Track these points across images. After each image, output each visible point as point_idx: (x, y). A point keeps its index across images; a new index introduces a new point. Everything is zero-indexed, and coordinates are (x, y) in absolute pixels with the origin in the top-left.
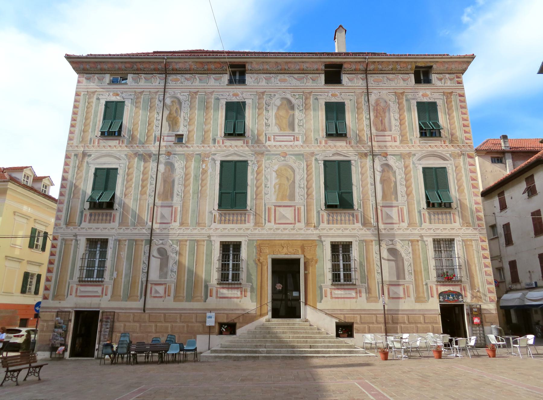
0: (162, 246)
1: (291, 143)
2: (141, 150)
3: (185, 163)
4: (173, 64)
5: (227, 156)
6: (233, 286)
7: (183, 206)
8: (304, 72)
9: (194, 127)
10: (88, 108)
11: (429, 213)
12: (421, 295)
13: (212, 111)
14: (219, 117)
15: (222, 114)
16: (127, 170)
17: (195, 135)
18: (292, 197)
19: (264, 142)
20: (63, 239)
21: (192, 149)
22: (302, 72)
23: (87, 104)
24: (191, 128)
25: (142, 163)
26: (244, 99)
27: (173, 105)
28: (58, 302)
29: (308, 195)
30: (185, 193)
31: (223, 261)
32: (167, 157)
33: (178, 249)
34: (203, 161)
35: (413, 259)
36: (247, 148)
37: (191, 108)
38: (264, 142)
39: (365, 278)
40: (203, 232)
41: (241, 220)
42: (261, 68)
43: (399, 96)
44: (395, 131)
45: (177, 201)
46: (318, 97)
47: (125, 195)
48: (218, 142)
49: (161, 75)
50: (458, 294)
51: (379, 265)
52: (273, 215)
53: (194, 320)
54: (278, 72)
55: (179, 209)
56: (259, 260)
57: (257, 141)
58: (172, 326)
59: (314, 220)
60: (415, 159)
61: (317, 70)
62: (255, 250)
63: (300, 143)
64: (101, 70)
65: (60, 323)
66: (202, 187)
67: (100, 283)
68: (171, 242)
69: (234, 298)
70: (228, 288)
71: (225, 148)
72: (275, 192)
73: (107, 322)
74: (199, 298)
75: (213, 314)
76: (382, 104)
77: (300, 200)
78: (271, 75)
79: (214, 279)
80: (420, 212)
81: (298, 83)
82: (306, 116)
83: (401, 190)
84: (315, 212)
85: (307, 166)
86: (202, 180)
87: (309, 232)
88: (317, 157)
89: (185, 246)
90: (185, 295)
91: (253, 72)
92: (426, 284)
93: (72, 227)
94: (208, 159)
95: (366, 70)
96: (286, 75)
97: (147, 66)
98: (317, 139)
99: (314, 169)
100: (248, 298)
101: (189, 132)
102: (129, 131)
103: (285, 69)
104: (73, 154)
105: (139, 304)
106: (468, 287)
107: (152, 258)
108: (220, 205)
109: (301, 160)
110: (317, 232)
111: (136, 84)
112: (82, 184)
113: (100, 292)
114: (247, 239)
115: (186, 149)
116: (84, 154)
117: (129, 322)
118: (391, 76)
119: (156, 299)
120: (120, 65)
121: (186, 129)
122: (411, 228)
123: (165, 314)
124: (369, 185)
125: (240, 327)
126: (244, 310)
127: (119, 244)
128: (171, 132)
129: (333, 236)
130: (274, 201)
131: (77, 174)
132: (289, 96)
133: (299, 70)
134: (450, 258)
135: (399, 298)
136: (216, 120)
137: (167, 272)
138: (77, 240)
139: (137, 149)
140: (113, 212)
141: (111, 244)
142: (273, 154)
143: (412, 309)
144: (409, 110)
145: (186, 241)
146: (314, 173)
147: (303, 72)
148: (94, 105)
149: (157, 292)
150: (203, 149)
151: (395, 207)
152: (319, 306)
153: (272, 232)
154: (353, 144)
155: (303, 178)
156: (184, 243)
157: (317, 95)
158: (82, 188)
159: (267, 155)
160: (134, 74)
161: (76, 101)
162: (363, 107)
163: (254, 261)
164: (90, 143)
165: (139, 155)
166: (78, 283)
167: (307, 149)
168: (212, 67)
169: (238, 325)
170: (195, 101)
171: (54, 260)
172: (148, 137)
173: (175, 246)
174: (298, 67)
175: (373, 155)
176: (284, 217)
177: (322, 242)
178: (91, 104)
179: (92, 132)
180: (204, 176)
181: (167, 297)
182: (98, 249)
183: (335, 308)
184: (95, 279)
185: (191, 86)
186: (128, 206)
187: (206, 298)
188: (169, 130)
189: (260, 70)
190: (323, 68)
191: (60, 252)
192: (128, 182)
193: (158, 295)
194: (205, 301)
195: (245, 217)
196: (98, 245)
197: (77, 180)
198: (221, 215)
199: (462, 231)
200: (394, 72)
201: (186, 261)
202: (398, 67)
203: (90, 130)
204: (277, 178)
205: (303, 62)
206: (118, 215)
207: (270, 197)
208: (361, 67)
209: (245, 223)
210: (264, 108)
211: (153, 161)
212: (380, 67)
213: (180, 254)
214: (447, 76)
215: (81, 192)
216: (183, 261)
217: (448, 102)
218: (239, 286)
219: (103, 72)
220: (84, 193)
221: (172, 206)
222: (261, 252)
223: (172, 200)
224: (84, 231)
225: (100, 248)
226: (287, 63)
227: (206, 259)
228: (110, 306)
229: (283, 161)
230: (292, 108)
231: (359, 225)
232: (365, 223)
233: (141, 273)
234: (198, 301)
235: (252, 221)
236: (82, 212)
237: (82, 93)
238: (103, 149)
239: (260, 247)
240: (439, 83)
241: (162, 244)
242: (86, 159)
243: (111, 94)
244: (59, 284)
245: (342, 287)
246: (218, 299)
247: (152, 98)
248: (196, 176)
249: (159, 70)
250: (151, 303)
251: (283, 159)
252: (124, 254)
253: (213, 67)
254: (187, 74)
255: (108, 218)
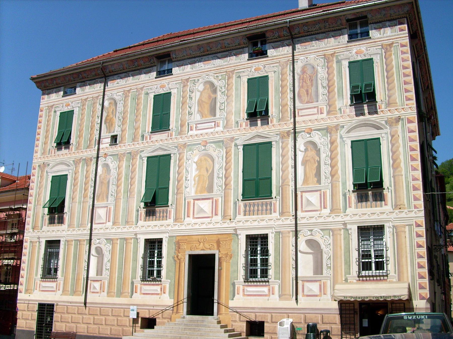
0: (98, 245)
1: (212, 130)
3: (118, 163)
9: (127, 126)
10: (48, 121)
18: (210, 189)
20: (31, 242)
29: (226, 185)
30: (117, 192)
46: (241, 75)
56: (177, 257)
59: (231, 212)
60: (343, 132)
62: (174, 247)
63: (220, 129)
66: (131, 185)
71: (151, 144)
72: (195, 184)
74: (127, 294)
76: (309, 72)
77: (217, 191)
80: (345, 195)
85: (227, 153)
86: (132, 179)
87: (226, 225)
90: (116, 291)
98: (237, 123)
99: (233, 156)
101: (122, 131)
104: (37, 165)
109: (220, 147)
111: (83, 92)
113: (55, 287)
114: (167, 235)
119: (94, 294)
121: (120, 129)
122: (333, 215)
123: (100, 308)
130: (193, 194)
132: (212, 79)
149: (95, 288)
153: (190, 227)
155: (221, 168)
157: (240, 72)
165: (83, 160)
172: (90, 141)
181: (102, 293)
187: (132, 294)
193: (96, 291)
194: (131, 297)
204: (197, 169)
207: (191, 190)
218: (160, 283)
222: (179, 248)
224: (44, 233)
233: (83, 270)
234: (126, 297)
236: (43, 217)
238: (58, 158)
241: (99, 243)
248: (126, 175)
251: (203, 148)
254: (122, 73)
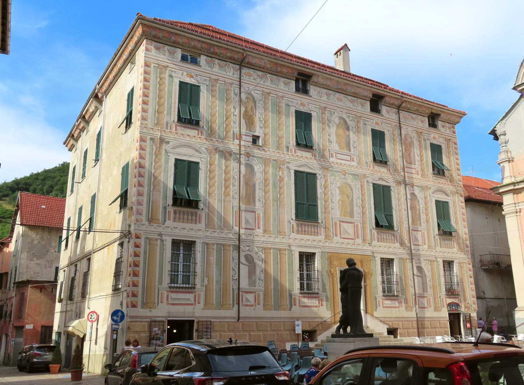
0: (248, 253)
1: (349, 163)
2: (221, 146)
3: (264, 167)
4: (250, 57)
5: (299, 166)
6: (312, 296)
7: (265, 213)
8: (357, 96)
9: (269, 130)
10: (160, 85)
11: (440, 238)
12: (437, 305)
13: (284, 117)
14: (290, 124)
15: (292, 121)
16: (209, 166)
17: (270, 139)
18: (352, 215)
19: (328, 158)
20: (147, 238)
21: (268, 153)
22: (355, 95)
23: (158, 79)
24: (267, 131)
25: (224, 161)
26: (311, 111)
27: (248, 102)
28: (148, 310)
29: (363, 214)
30: (266, 199)
31: (300, 271)
32: (247, 159)
33: (263, 256)
34: (280, 168)
35: (432, 276)
36: (315, 162)
37: (265, 109)
38: (328, 158)
39: (403, 290)
40: (284, 241)
41: (192, 220)
42: (325, 83)
43: (420, 134)
44: (417, 166)
45: (259, 205)
46: (367, 123)
47: (209, 195)
48: (291, 150)
49: (234, 65)
50: (457, 305)
51: (412, 280)
52: (338, 230)
53: (282, 329)
54: (338, 90)
55: (261, 215)
56: (330, 271)
57: (323, 156)
58: (264, 335)
59: (368, 237)
60: (430, 191)
61: (366, 97)
62: (327, 262)
63: (354, 164)
64: (174, 42)
65: (157, 334)
66: (280, 195)
67: (192, 290)
68: (256, 249)
69: (313, 306)
70: (308, 297)
71: (297, 158)
72: (339, 207)
73: (206, 332)
74: (285, 307)
75: (299, 323)
76: (409, 140)
77: (357, 218)
78: (331, 92)
79: (297, 288)
80: (434, 237)
81: (351, 105)
82: (358, 138)
83: (423, 217)
84: (369, 230)
85: (362, 187)
86: (280, 188)
87: (365, 248)
88: (368, 179)
89: (269, 254)
90: (273, 304)
91: (316, 84)
92: (440, 297)
93: (155, 225)
94: (283, 167)
95: (400, 106)
96: (342, 95)
97: (224, 52)
98: (367, 162)
99: (366, 190)
100: (324, 307)
101: (265, 135)
102: (208, 122)
103: (343, 90)
104: (148, 137)
105: (232, 313)
106: (462, 300)
107: (241, 264)
108: (297, 216)
109: (356, 180)
110: (370, 248)
111: (210, 69)
112: (162, 174)
113: (192, 299)
114: (320, 251)
115: (263, 152)
116: (162, 141)
117: (225, 331)
118: (414, 116)
119: (248, 308)
120: (196, 43)
121: (262, 132)
122: (429, 250)
123: (257, 322)
124: (403, 210)
125: (320, 334)
126: (321, 318)
127: (207, 248)
128: (248, 132)
129: (382, 253)
130: (338, 216)
131: (156, 162)
132: (345, 116)
133: (353, 93)
134: (390, 274)
135: (424, 308)
136: (288, 127)
137: (255, 280)
138: (162, 241)
139: (216, 144)
140: (199, 212)
141: (199, 247)
142: (336, 171)
143: (432, 316)
144: (426, 148)
145: (270, 249)
146: (366, 194)
147: (355, 95)
148: (167, 82)
149: (247, 300)
150: (278, 155)
151: (420, 231)
152: (376, 314)
153: (338, 245)
154: (391, 172)
155: (358, 198)
156: (268, 251)
157: (366, 120)
158: (162, 180)
159: (331, 170)
160: (207, 56)
161: (145, 72)
162: (397, 139)
163: (327, 272)
164: (167, 128)
165: (220, 151)
166: (169, 290)
167: (360, 170)
168: (285, 70)
169: (318, 332)
170: (268, 103)
171: (139, 262)
172: (227, 132)
173: (261, 253)
174: (353, 91)
175: (406, 185)
176: (347, 232)
177: (374, 257)
178: (164, 80)
179: (167, 114)
180: (282, 183)
181: (257, 306)
182: (182, 251)
183: (386, 316)
184: (179, 285)
185: (263, 85)
186: (213, 207)
187: (291, 307)
188: (247, 129)
189: (323, 85)
190: (371, 96)
191: (145, 253)
192: (210, 180)
193: (249, 304)
194: (290, 310)
195: (318, 230)
196: (184, 247)
197: (156, 169)
198: (298, 224)
199: (458, 255)
200: (416, 112)
201: (271, 271)
202: (420, 109)
203: (165, 112)
204: (340, 194)
205: (358, 87)
206: (203, 216)
207: (336, 213)
208: (397, 103)
209: (196, 223)
210: (327, 123)
211: (234, 160)
212: (409, 106)
213: (265, 262)
214: (447, 124)
215: (162, 186)
216: (269, 270)
217: (448, 147)
218: (317, 296)
219: (175, 44)
220: (166, 187)
221: (254, 212)
222: (331, 264)
223: (255, 206)
224: (169, 230)
225: (184, 251)
226: (346, 84)
227: (289, 269)
228: (203, 315)
229: (344, 179)
230: (348, 129)
231: (398, 245)
232: (402, 244)
233: (231, 279)
234: (284, 309)
235: (323, 234)
236: (165, 208)
237: (153, 65)
238: (182, 138)
239: (330, 259)
240: (442, 130)
241: (249, 250)
242: (164, 146)
243: (185, 74)
244: (147, 290)
245: (390, 298)
246: (301, 308)
247: (227, 90)
248: (274, 184)
249: (234, 59)
250: (245, 312)
251: (343, 177)
252: (213, 259)
253: (286, 71)
254: (259, 70)
255: (194, 218)
